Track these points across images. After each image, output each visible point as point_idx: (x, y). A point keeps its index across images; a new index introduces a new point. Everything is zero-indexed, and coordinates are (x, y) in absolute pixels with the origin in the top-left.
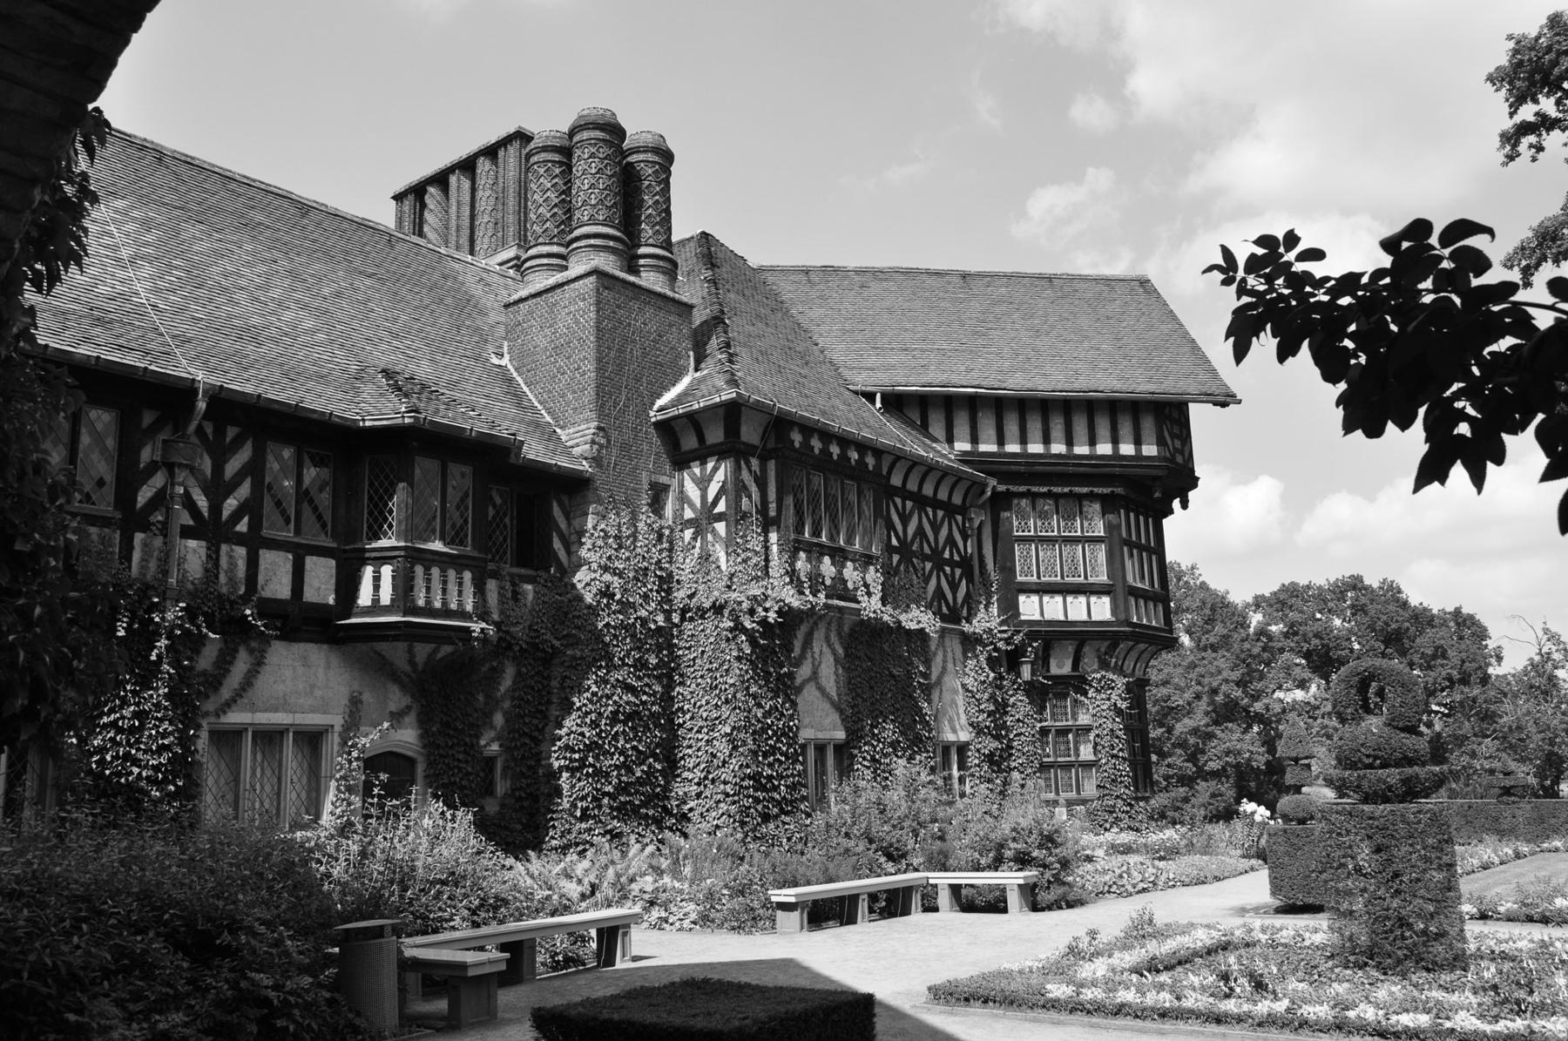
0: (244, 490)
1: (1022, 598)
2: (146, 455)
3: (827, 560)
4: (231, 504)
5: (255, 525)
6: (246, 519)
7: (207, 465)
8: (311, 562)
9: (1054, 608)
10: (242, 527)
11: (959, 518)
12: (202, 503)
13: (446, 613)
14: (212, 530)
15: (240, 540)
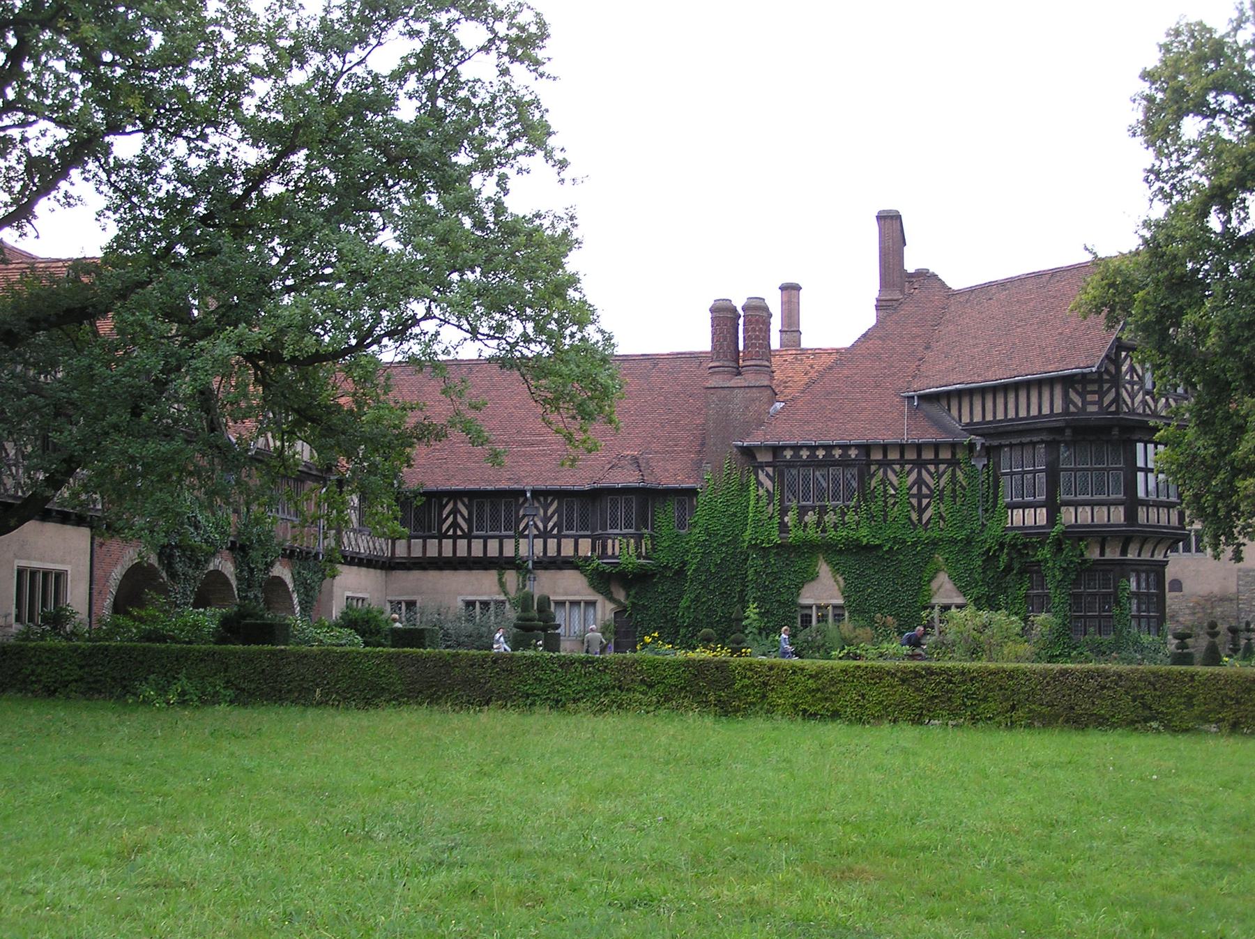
0: (555, 518)
2: (521, 513)
4: (551, 524)
7: (542, 512)
8: (580, 540)
10: (555, 532)
12: (541, 526)
14: (545, 535)
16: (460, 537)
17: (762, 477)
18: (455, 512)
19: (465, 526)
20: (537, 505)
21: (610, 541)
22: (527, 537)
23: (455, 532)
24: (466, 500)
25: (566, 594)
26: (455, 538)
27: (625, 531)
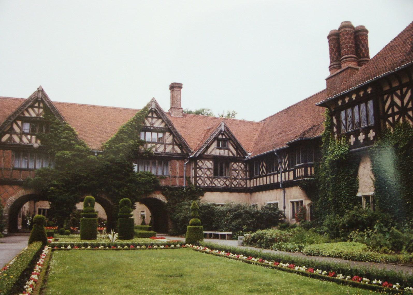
0: (287, 163)
4: (286, 165)
5: (289, 169)
10: (288, 169)
13: (300, 177)
14: (285, 171)
18: (263, 166)
19: (265, 171)
20: (282, 157)
21: (297, 170)
24: (265, 160)
25: (294, 198)
27: (302, 164)
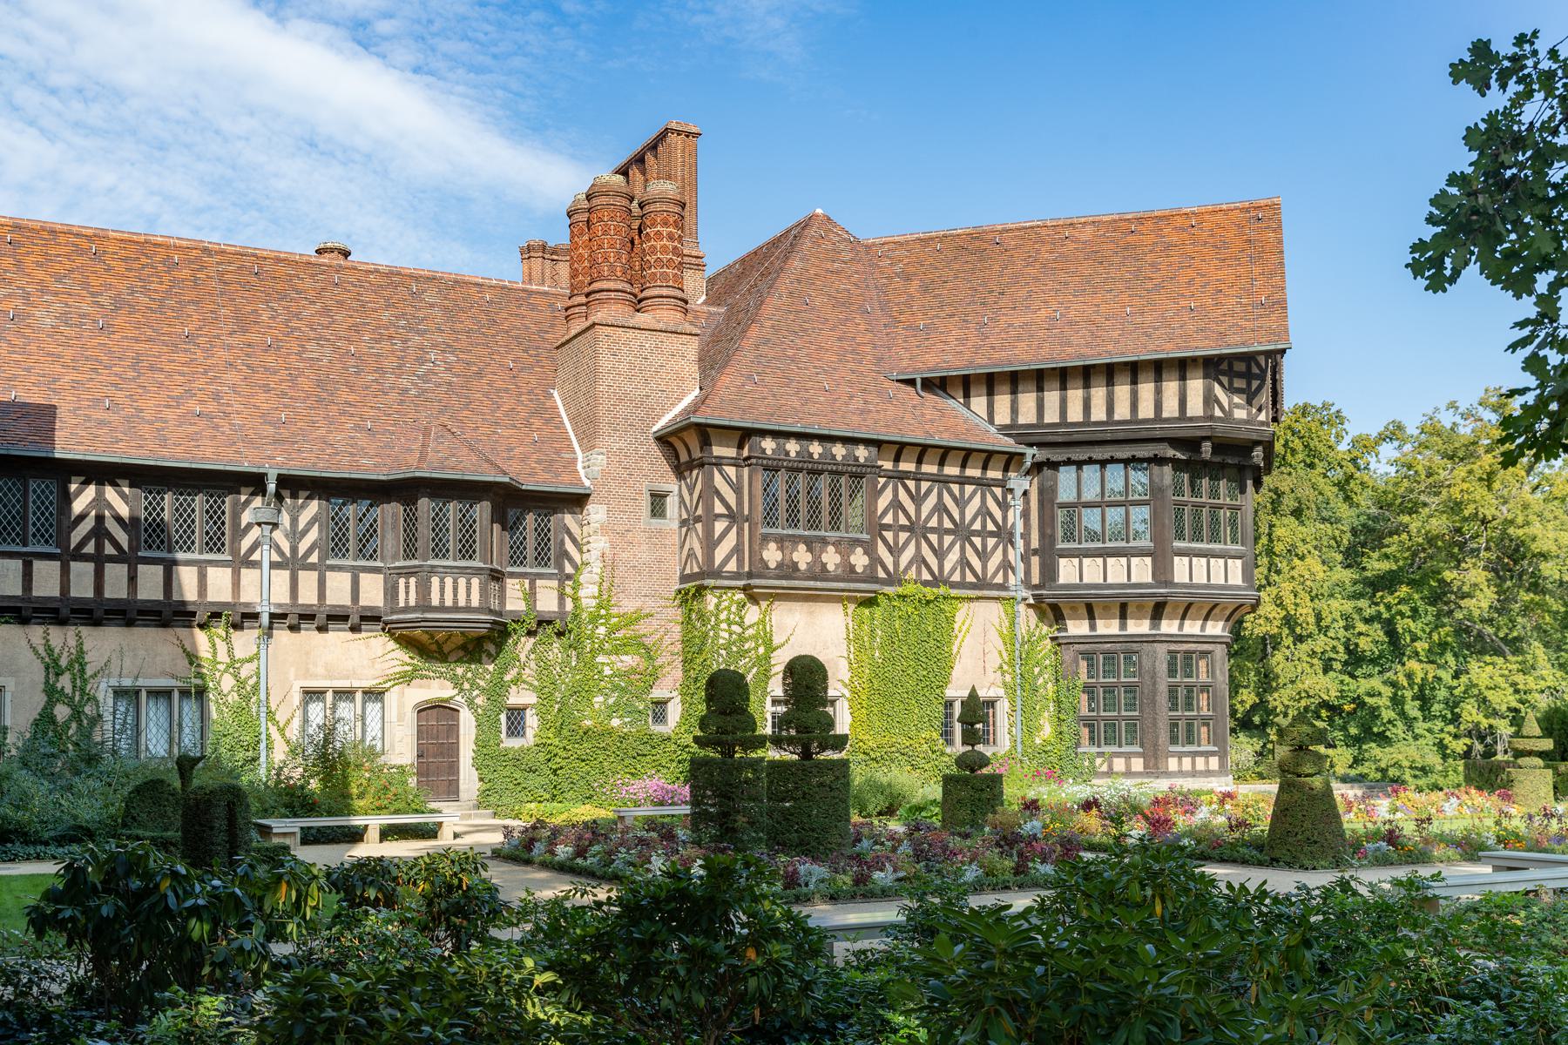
0: (313, 535)
1: (1063, 562)
3: (802, 547)
6: (316, 554)
9: (1092, 571)
10: (314, 558)
11: (998, 491)
13: (456, 608)
14: (292, 564)
15: (312, 567)
16: (111, 559)
17: (718, 480)
21: (435, 581)
22: (256, 565)
23: (99, 547)
25: (331, 678)
26: (99, 560)
